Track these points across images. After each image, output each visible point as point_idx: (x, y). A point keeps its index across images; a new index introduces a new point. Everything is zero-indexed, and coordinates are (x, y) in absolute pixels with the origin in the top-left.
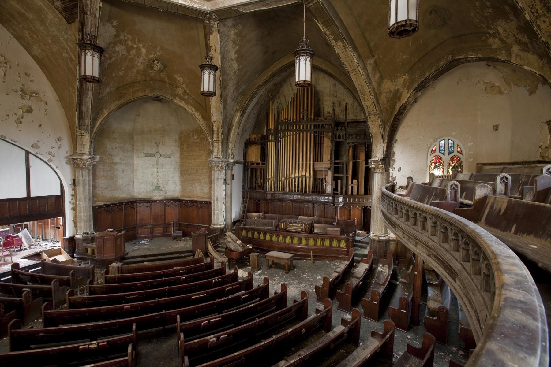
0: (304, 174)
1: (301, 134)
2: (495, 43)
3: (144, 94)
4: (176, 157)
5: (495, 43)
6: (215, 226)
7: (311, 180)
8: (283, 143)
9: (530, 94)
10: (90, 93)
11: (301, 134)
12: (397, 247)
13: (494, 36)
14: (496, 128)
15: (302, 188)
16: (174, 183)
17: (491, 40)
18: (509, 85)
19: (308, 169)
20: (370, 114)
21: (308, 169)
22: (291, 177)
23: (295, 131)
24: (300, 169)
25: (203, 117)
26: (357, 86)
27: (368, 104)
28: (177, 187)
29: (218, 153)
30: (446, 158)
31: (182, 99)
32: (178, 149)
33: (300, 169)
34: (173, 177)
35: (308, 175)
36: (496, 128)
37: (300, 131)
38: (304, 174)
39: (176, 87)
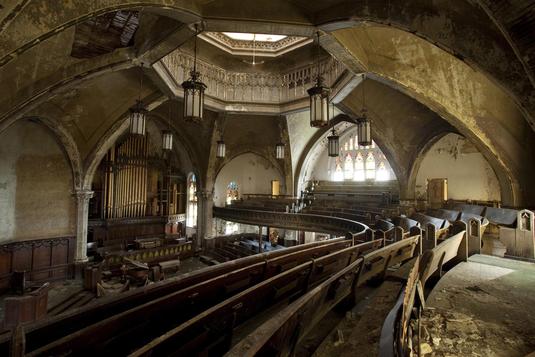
0: (139, 201)
1: (137, 168)
2: (265, 151)
3: (32, 115)
4: (12, 187)
5: (265, 151)
6: (84, 261)
7: (145, 206)
8: (120, 174)
9: (266, 169)
10: (22, 114)
11: (137, 168)
12: (216, 241)
13: (266, 149)
14: (250, 179)
15: (134, 214)
16: (8, 222)
17: (264, 150)
18: (258, 163)
19: (143, 198)
20: (210, 167)
21: (143, 198)
22: (130, 203)
23: (132, 165)
24: (136, 198)
25: (78, 148)
26: (211, 152)
27: (212, 162)
28: (10, 227)
29: (88, 184)
30: (233, 191)
31: (65, 126)
32: (15, 176)
33: (136, 198)
34: (7, 214)
35: (142, 202)
36: (250, 179)
37: (133, 165)
38: (139, 201)
39: (67, 114)
